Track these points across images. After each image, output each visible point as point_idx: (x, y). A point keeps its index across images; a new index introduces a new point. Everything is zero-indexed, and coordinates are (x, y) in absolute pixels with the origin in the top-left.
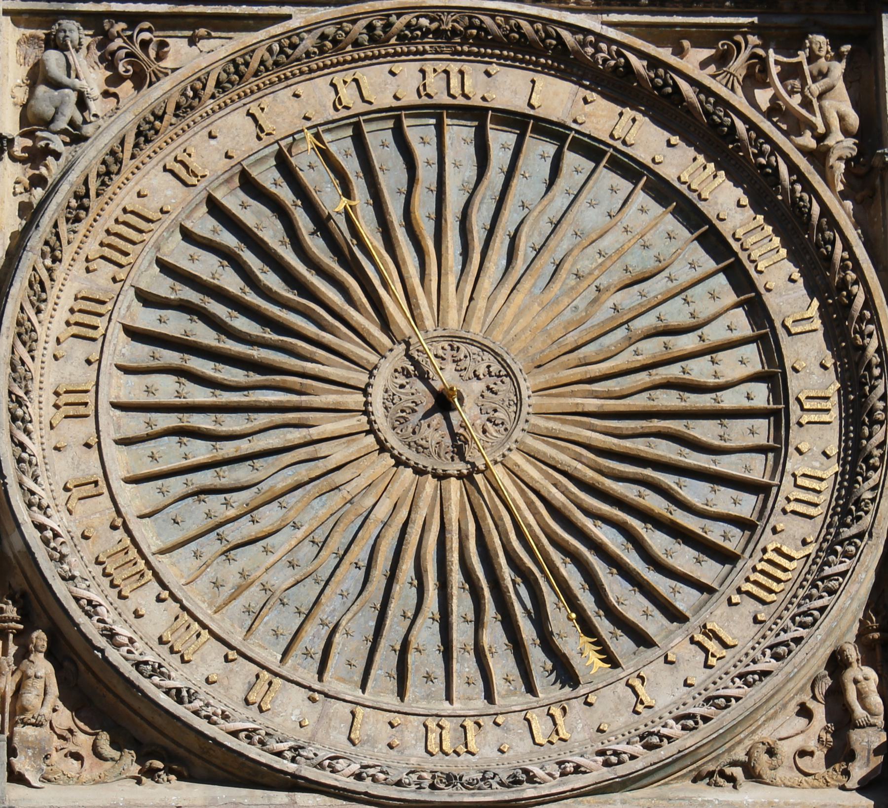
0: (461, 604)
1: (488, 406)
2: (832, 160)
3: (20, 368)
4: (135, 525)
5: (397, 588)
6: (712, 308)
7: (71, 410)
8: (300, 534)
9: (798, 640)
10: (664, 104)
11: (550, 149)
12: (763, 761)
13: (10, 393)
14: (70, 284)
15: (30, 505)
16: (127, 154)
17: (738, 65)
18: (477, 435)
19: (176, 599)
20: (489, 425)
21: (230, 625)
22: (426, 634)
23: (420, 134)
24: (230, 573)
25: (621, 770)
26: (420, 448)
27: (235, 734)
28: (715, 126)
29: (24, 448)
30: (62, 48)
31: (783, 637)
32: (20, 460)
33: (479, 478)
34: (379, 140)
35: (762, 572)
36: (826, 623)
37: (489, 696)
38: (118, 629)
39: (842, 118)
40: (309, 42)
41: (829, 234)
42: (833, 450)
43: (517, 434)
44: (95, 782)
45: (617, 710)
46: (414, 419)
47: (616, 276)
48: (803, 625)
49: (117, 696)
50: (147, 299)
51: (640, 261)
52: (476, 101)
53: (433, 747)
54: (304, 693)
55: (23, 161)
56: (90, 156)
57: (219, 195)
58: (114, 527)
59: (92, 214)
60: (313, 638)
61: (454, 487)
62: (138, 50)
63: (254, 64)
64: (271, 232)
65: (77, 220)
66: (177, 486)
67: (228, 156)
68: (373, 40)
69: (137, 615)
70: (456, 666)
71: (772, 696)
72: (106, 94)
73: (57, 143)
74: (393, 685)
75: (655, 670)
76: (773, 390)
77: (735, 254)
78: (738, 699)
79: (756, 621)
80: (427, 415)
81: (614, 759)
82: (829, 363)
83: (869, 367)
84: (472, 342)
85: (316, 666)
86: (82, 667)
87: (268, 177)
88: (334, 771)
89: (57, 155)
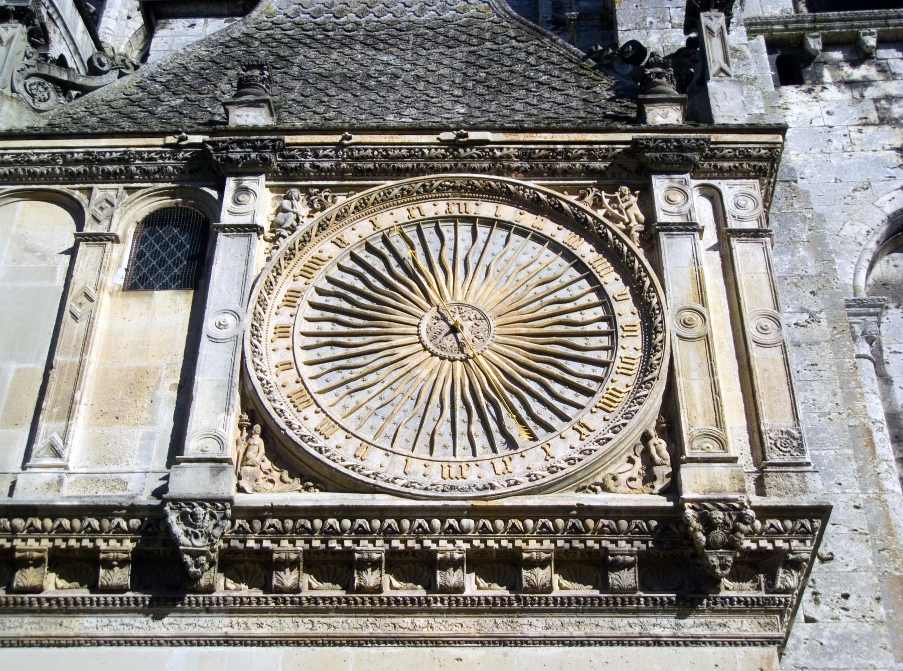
0: (461, 414)
1: (475, 331)
2: (633, 232)
3: (258, 315)
4: (307, 381)
5: (430, 407)
6: (579, 292)
7: (281, 335)
8: (385, 385)
9: (624, 425)
11: (506, 233)
12: (611, 484)
13: (253, 325)
14: (285, 285)
15: (257, 370)
16: (313, 234)
17: (589, 198)
18: (470, 343)
19: (324, 412)
20: (476, 339)
21: (350, 424)
22: (444, 428)
23: (447, 229)
24: (351, 402)
25: (537, 483)
26: (443, 348)
27: (347, 467)
28: (578, 219)
29: (256, 347)
30: (290, 199)
31: (618, 423)
32: (254, 352)
33: (470, 361)
35: (607, 398)
36: (637, 417)
37: (474, 454)
38: (293, 422)
39: (636, 216)
40: (396, 191)
41: (632, 258)
42: (639, 346)
43: (489, 342)
44: (279, 492)
45: (537, 459)
46: (440, 337)
47: (536, 280)
48: (626, 418)
49: (292, 453)
50: (320, 292)
51: (545, 275)
52: (472, 214)
53: (446, 475)
54: (384, 452)
55: (270, 241)
57: (356, 252)
58: (297, 382)
59: (297, 258)
60: (390, 430)
61: (459, 365)
62: (323, 199)
63: (372, 199)
64: (379, 266)
65: (290, 259)
66: (329, 366)
67: (360, 237)
68: (425, 191)
69: (305, 419)
70: (458, 441)
71: (613, 450)
72: (309, 216)
73: (285, 233)
74: (428, 450)
75: (556, 442)
76: (610, 325)
77: (590, 270)
78: (595, 451)
79: (605, 420)
80: (446, 335)
81: (534, 478)
82: (636, 310)
83: (654, 310)
84: (468, 306)
85: (390, 442)
86: (277, 441)
87: (379, 245)
88: (395, 483)
89: (284, 237)
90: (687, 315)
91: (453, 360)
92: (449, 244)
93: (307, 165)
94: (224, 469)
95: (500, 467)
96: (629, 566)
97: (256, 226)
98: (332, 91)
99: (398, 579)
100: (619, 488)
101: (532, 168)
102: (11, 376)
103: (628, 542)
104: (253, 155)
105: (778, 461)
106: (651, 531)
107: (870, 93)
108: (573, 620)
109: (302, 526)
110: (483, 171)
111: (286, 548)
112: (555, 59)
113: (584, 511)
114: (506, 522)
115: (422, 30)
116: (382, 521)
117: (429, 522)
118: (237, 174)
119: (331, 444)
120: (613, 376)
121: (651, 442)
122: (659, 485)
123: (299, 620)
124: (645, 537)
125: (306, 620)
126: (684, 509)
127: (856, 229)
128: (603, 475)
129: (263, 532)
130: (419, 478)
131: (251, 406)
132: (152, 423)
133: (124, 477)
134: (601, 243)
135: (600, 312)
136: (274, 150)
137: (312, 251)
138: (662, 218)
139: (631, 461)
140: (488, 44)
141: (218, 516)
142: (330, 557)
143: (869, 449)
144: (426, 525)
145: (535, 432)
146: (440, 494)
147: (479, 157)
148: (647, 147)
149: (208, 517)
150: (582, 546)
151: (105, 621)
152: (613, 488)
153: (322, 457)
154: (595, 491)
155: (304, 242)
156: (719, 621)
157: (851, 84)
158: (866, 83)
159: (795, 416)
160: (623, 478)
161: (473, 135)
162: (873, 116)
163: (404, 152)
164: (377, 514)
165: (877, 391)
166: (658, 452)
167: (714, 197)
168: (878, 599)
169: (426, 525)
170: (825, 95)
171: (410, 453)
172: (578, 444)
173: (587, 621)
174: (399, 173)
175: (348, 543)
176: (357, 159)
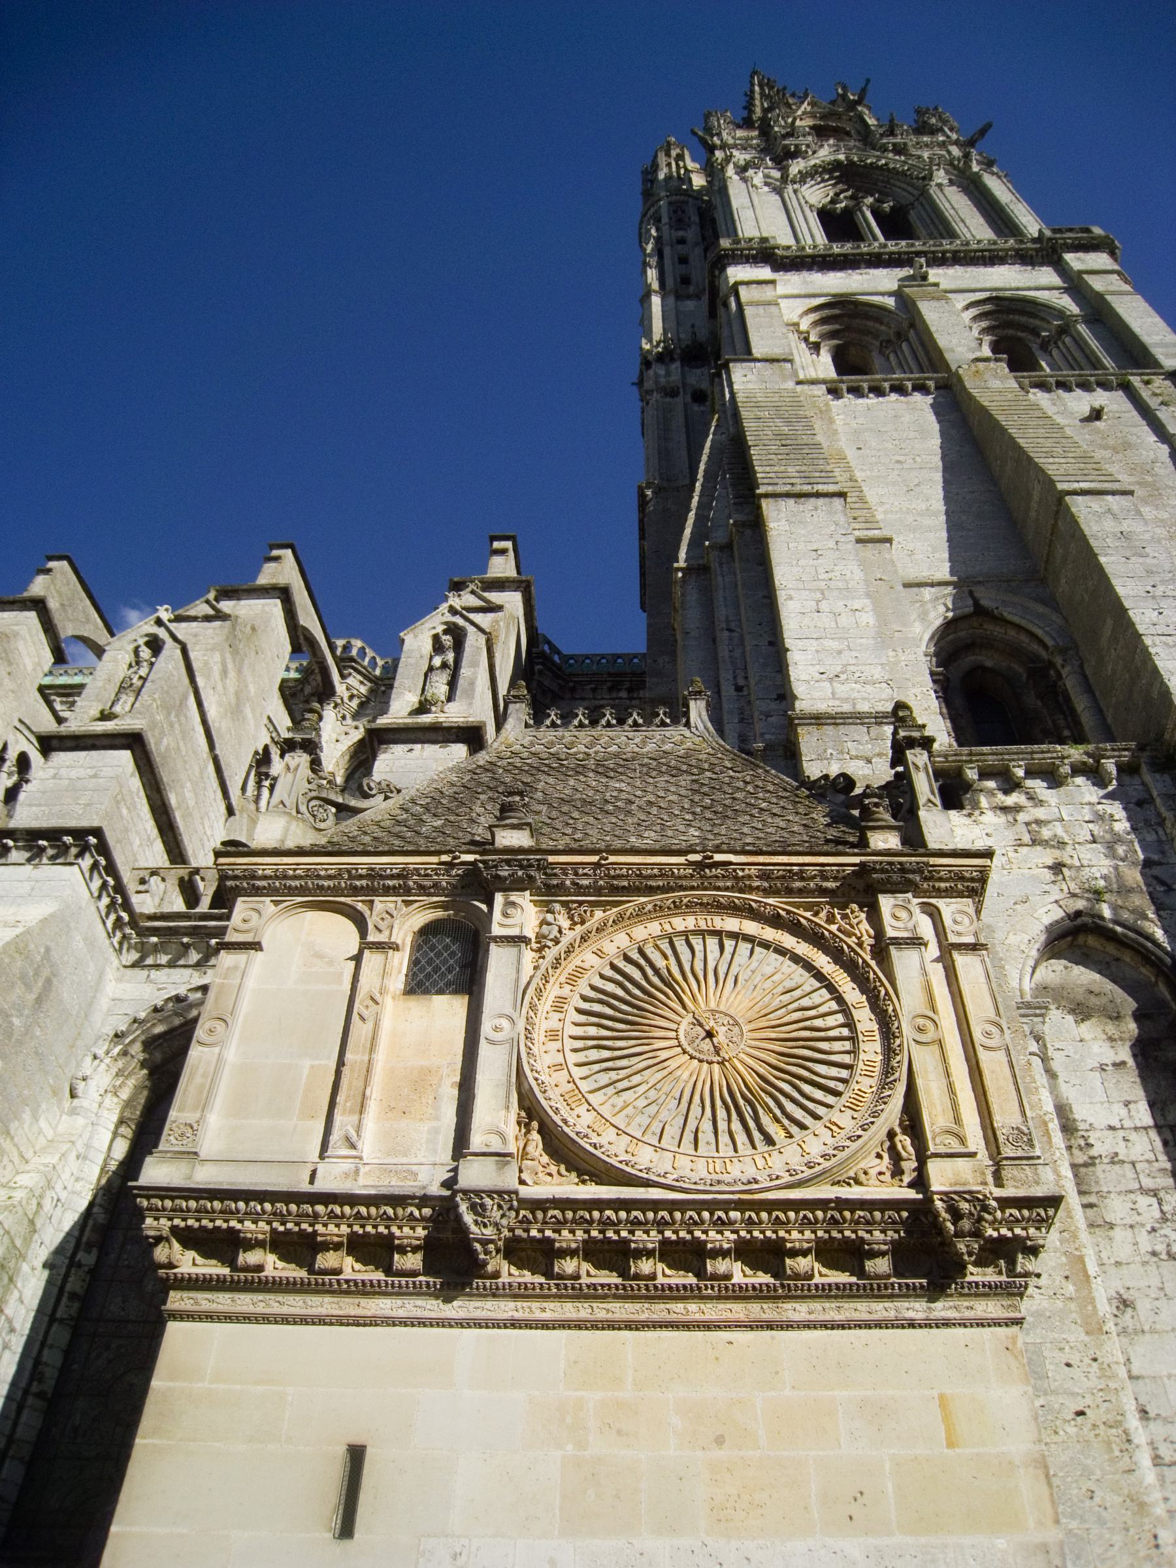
0: (721, 1113)
4: (578, 1081)
6: (820, 1000)
8: (650, 1085)
9: (872, 1123)
10: (795, 928)
11: (750, 946)
12: (862, 1177)
14: (553, 991)
16: (576, 945)
17: (823, 914)
21: (619, 1121)
22: (706, 1125)
23: (696, 942)
24: (619, 1101)
25: (797, 1177)
26: (700, 1052)
27: (621, 1162)
28: (816, 934)
30: (553, 913)
34: (680, 944)
36: (883, 1116)
37: (736, 1151)
40: (650, 907)
42: (879, 1051)
43: (742, 1046)
46: (697, 1041)
47: (780, 989)
50: (585, 999)
51: (789, 984)
52: (718, 928)
53: (711, 1170)
56: (562, 946)
57: (615, 962)
60: (656, 1127)
61: (716, 1067)
63: (628, 914)
66: (596, 1067)
69: (578, 1116)
73: (550, 944)
75: (810, 1138)
76: (851, 1030)
82: (873, 1017)
84: (721, 1012)
87: (635, 956)
90: (921, 1021)
91: (710, 1063)
92: (699, 955)
93: (568, 883)
94: (508, 1163)
95: (760, 1163)
96: (883, 1254)
97: (525, 937)
98: (576, 815)
99: (670, 1267)
100: (871, 1182)
101: (770, 887)
102: (306, 1072)
103: (882, 1232)
104: (520, 873)
105: (1012, 1155)
106: (902, 1222)
107: (1022, 817)
108: (833, 1305)
109: (582, 1217)
110: (727, 889)
111: (567, 1238)
112: (771, 788)
113: (842, 1204)
114: (770, 1214)
115: (646, 760)
116: (656, 1213)
117: (699, 1214)
118: (504, 890)
119: (603, 1140)
120: (858, 1078)
121: (897, 1139)
122: (907, 1179)
123: (580, 1305)
124: (898, 1227)
125: (586, 1305)
126: (933, 1201)
127: (1019, 938)
128: (855, 1169)
129: (545, 1222)
130: (687, 1173)
131: (527, 1104)
132: (437, 1118)
133: (414, 1168)
134: (837, 955)
135: (840, 1018)
136: (539, 869)
137: (575, 961)
138: (890, 933)
139: (879, 1156)
140: (708, 774)
141: (505, 1207)
142: (606, 1247)
143: (1045, 1138)
144: (696, 1217)
145: (790, 1129)
146: (708, 1188)
147: (723, 876)
148: (874, 869)
149: (495, 1207)
150: (839, 1236)
151: (399, 1302)
152: (865, 1182)
153: (597, 1153)
154: (849, 1184)
155: (568, 952)
156: (966, 1304)
157: (1004, 809)
158: (1017, 809)
159: (1023, 1113)
160: (873, 1172)
161: (718, 857)
162: (1026, 838)
163: (656, 871)
164: (650, 1207)
165: (1046, 1085)
166: (903, 1147)
167: (934, 914)
168: (1067, 1277)
169: (696, 1217)
170: (983, 818)
171: (677, 1149)
172: (830, 1141)
173: (846, 1305)
174: (651, 891)
175: (624, 1234)
176: (614, 877)
